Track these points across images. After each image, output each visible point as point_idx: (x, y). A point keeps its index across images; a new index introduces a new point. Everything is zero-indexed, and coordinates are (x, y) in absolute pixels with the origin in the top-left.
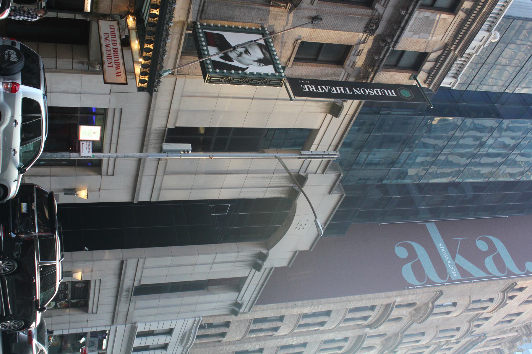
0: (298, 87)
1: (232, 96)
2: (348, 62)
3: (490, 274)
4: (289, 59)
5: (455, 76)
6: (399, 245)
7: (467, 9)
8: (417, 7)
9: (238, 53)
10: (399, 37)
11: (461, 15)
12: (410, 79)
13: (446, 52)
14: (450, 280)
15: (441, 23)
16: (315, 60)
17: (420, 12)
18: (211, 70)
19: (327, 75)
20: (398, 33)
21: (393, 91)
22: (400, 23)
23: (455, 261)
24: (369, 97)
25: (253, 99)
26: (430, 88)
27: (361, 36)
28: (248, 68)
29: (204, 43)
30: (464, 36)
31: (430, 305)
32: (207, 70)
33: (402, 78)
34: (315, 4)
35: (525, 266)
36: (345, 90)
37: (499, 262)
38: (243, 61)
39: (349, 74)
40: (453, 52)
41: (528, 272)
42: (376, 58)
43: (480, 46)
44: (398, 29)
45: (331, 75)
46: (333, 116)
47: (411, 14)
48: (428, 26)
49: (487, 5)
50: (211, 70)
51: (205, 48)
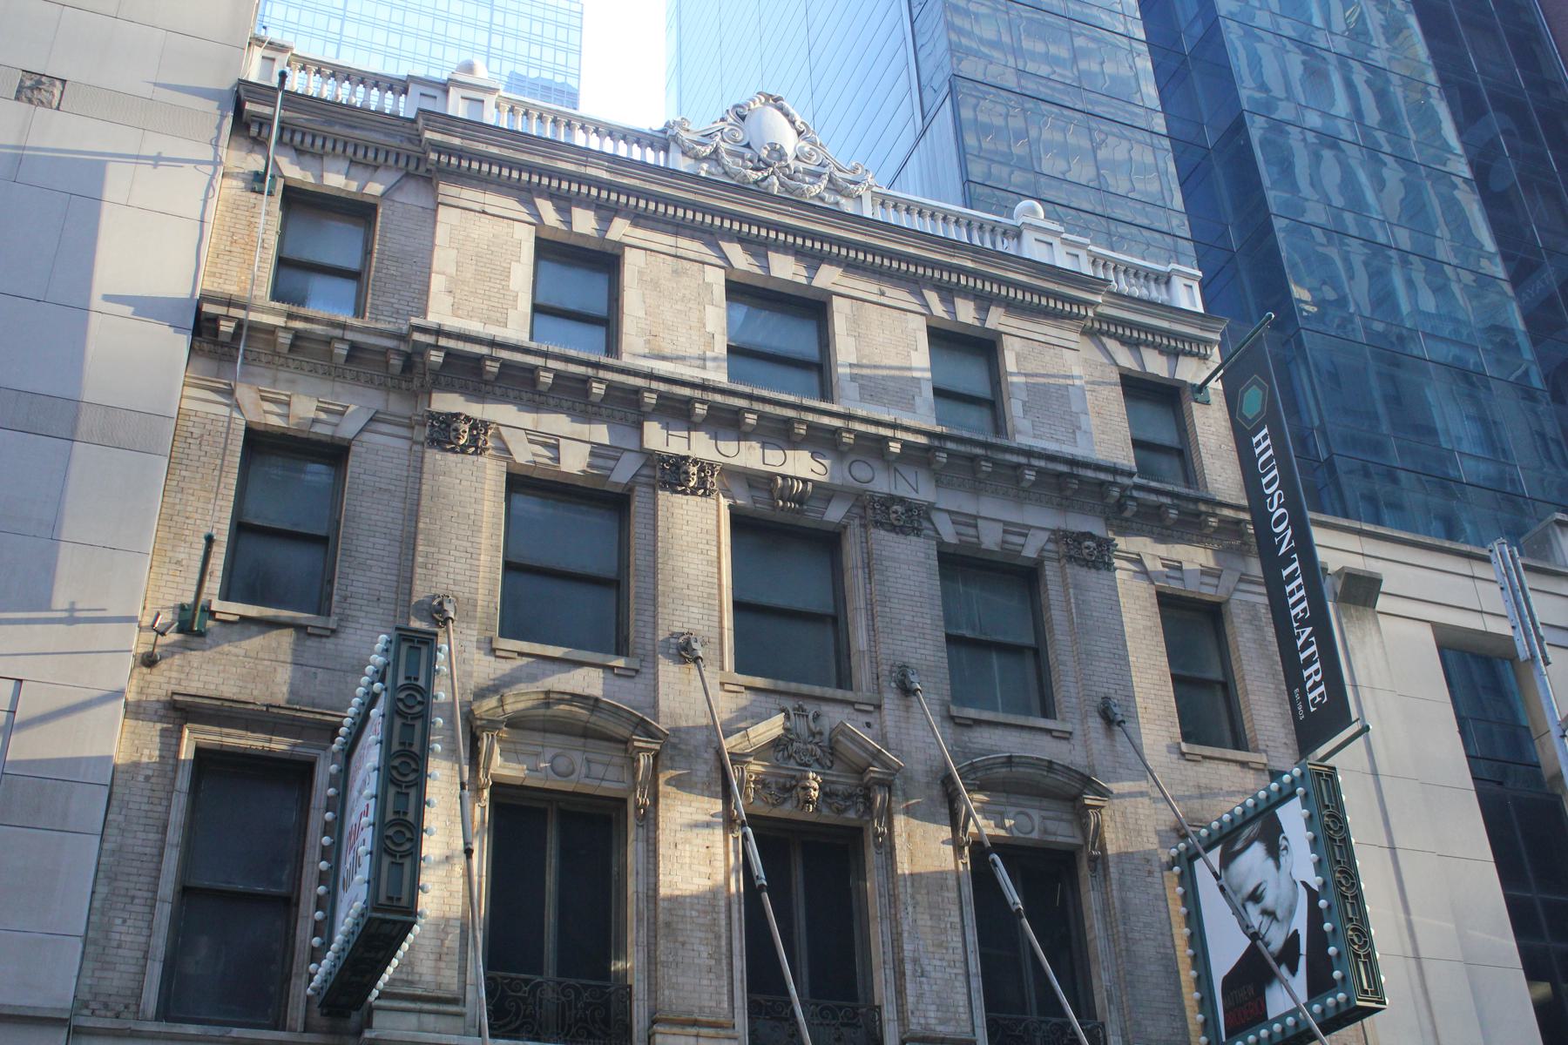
0: (1323, 718)
1: (1402, 916)
2: (1208, 592)
4: (1244, 764)
5: (1165, 280)
7: (979, 309)
8: (1005, 442)
9: (1266, 920)
10: (1098, 467)
11: (997, 319)
12: (1207, 403)
13: (1105, 327)
15: (1030, 367)
16: (1227, 687)
17: (1016, 431)
18: (1341, 996)
19: (1261, 643)
20: (1090, 473)
21: (1255, 440)
22: (1059, 475)
24: (1291, 503)
25: (1393, 849)
26: (1217, 337)
27: (1123, 573)
28: (1304, 883)
29: (1264, 1033)
30: (1049, 294)
32: (1343, 1009)
33: (1211, 426)
34: (1068, 727)
36: (1292, 577)
38: (1286, 905)
39: (1241, 580)
40: (1099, 309)
42: (1173, 513)
43: (1065, 242)
44: (1076, 476)
45: (1259, 629)
46: (1378, 592)
47: (1029, 453)
48: (1052, 397)
49: (955, 261)
50: (1341, 996)
51: (1277, 1027)
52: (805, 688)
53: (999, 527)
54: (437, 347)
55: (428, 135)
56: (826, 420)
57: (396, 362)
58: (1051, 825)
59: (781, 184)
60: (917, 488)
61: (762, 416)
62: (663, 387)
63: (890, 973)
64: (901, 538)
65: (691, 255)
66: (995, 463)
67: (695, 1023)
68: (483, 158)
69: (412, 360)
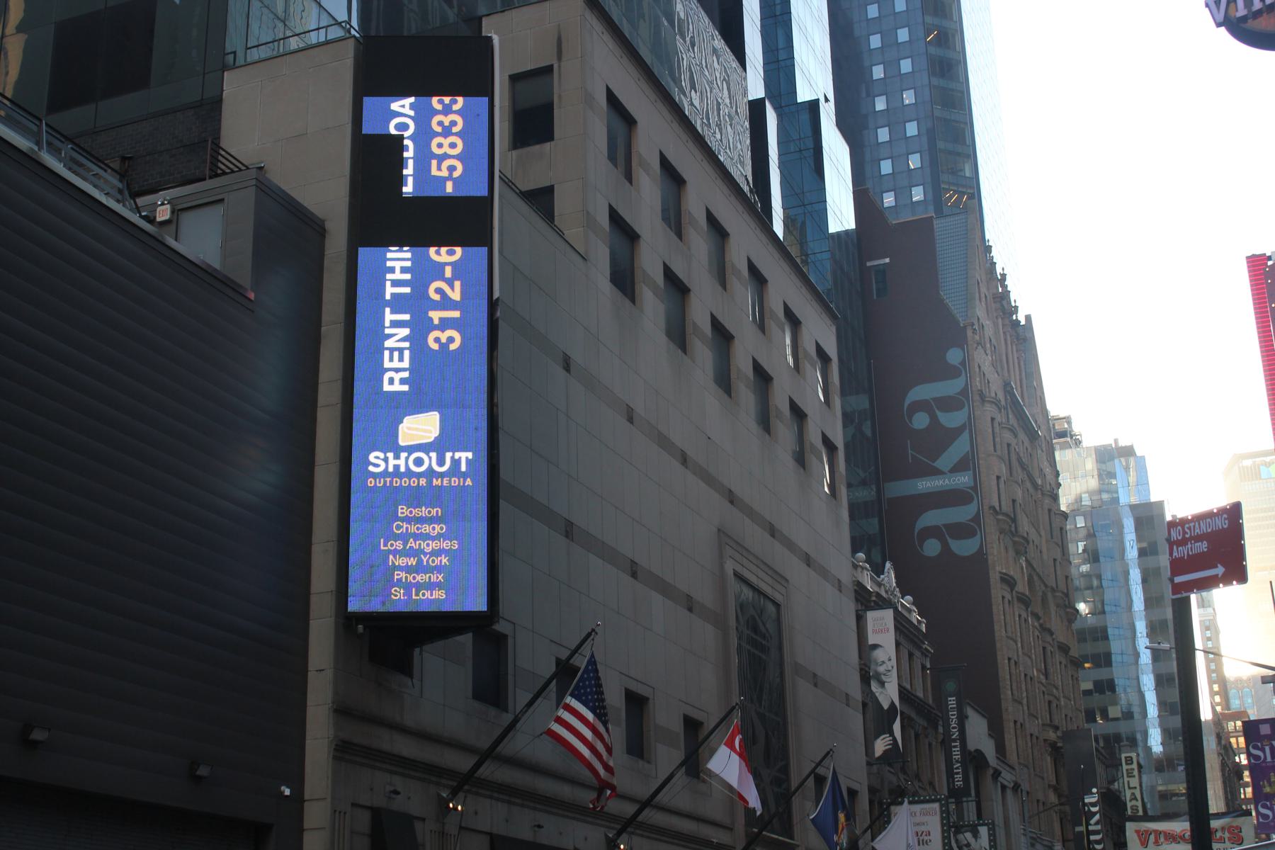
3: (964, 425)
6: (921, 546)
14: (975, 488)
23: (946, 470)
31: (1000, 517)
35: (954, 367)
37: (949, 404)
41: (963, 363)
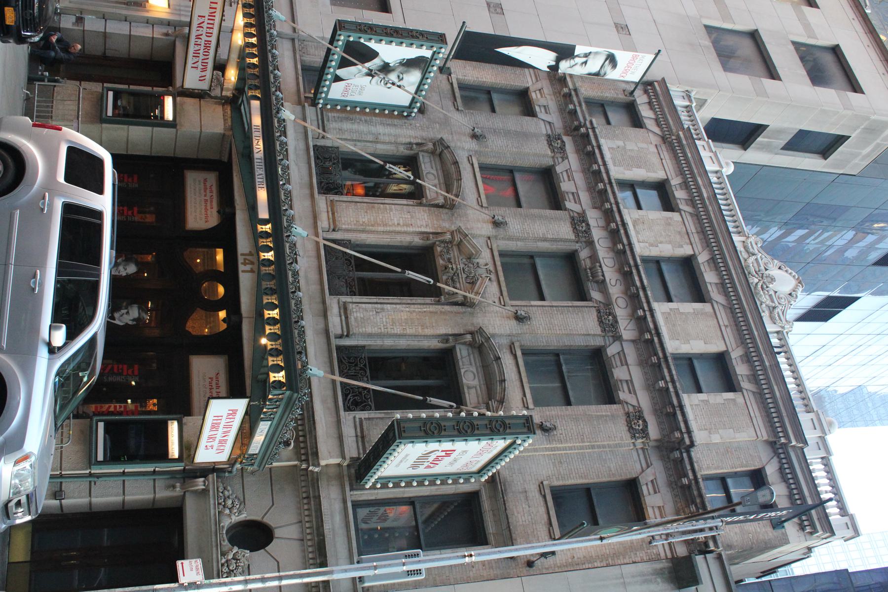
20: (680, 418)
52: (501, 274)
53: (628, 378)
54: (587, 129)
55: (681, 133)
56: (636, 278)
57: (576, 123)
58: (473, 391)
59: (757, 284)
60: (627, 330)
61: (624, 252)
62: (615, 209)
63: (375, 301)
64: (596, 323)
65: (692, 239)
66: (659, 366)
67: (333, 214)
68: (685, 155)
69: (577, 128)
